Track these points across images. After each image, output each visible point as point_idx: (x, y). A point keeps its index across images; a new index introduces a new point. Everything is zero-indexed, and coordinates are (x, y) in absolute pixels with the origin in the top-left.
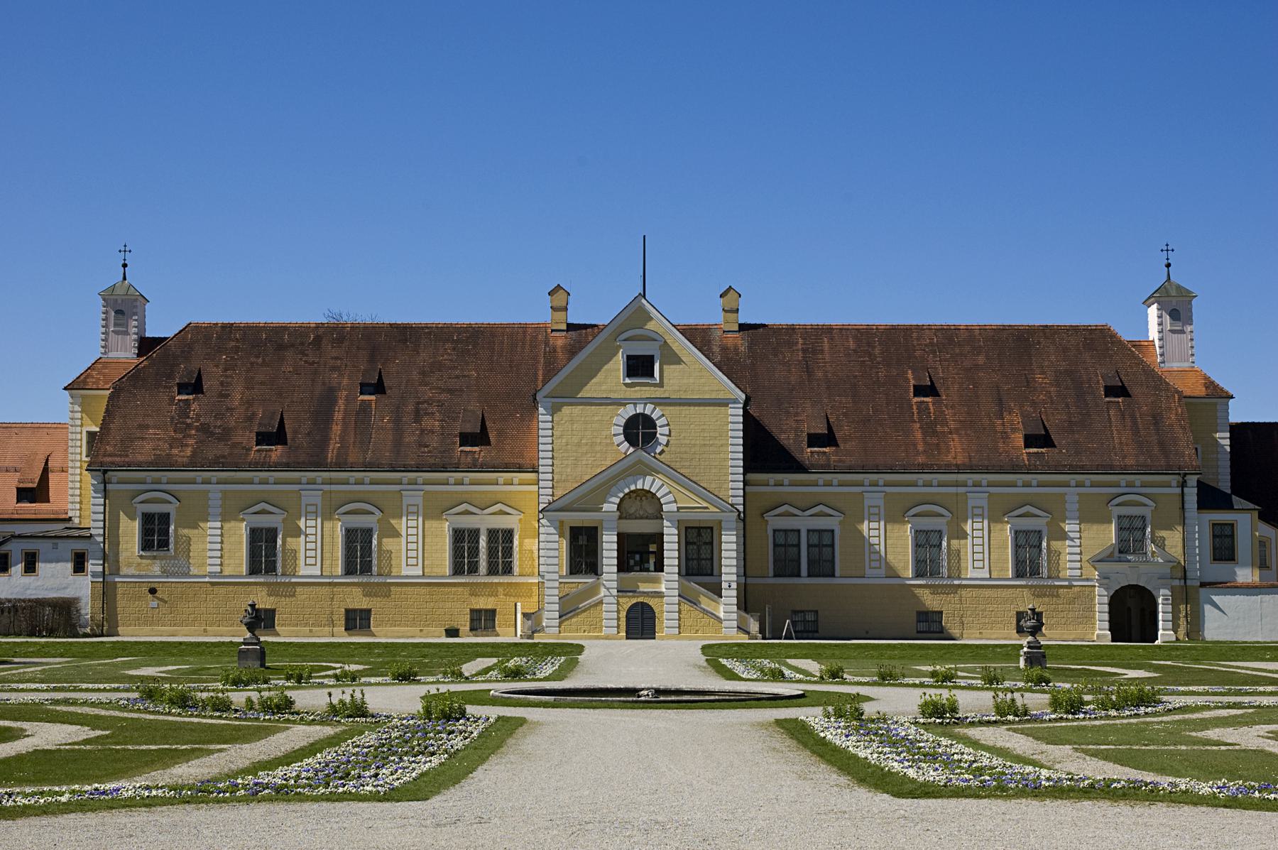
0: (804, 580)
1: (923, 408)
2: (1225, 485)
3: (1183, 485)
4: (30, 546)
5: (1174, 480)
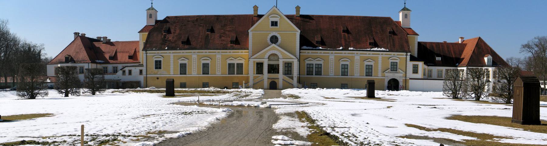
0: (314, 76)
1: (344, 35)
2: (416, 55)
3: (407, 55)
4: (130, 68)
5: (405, 54)
